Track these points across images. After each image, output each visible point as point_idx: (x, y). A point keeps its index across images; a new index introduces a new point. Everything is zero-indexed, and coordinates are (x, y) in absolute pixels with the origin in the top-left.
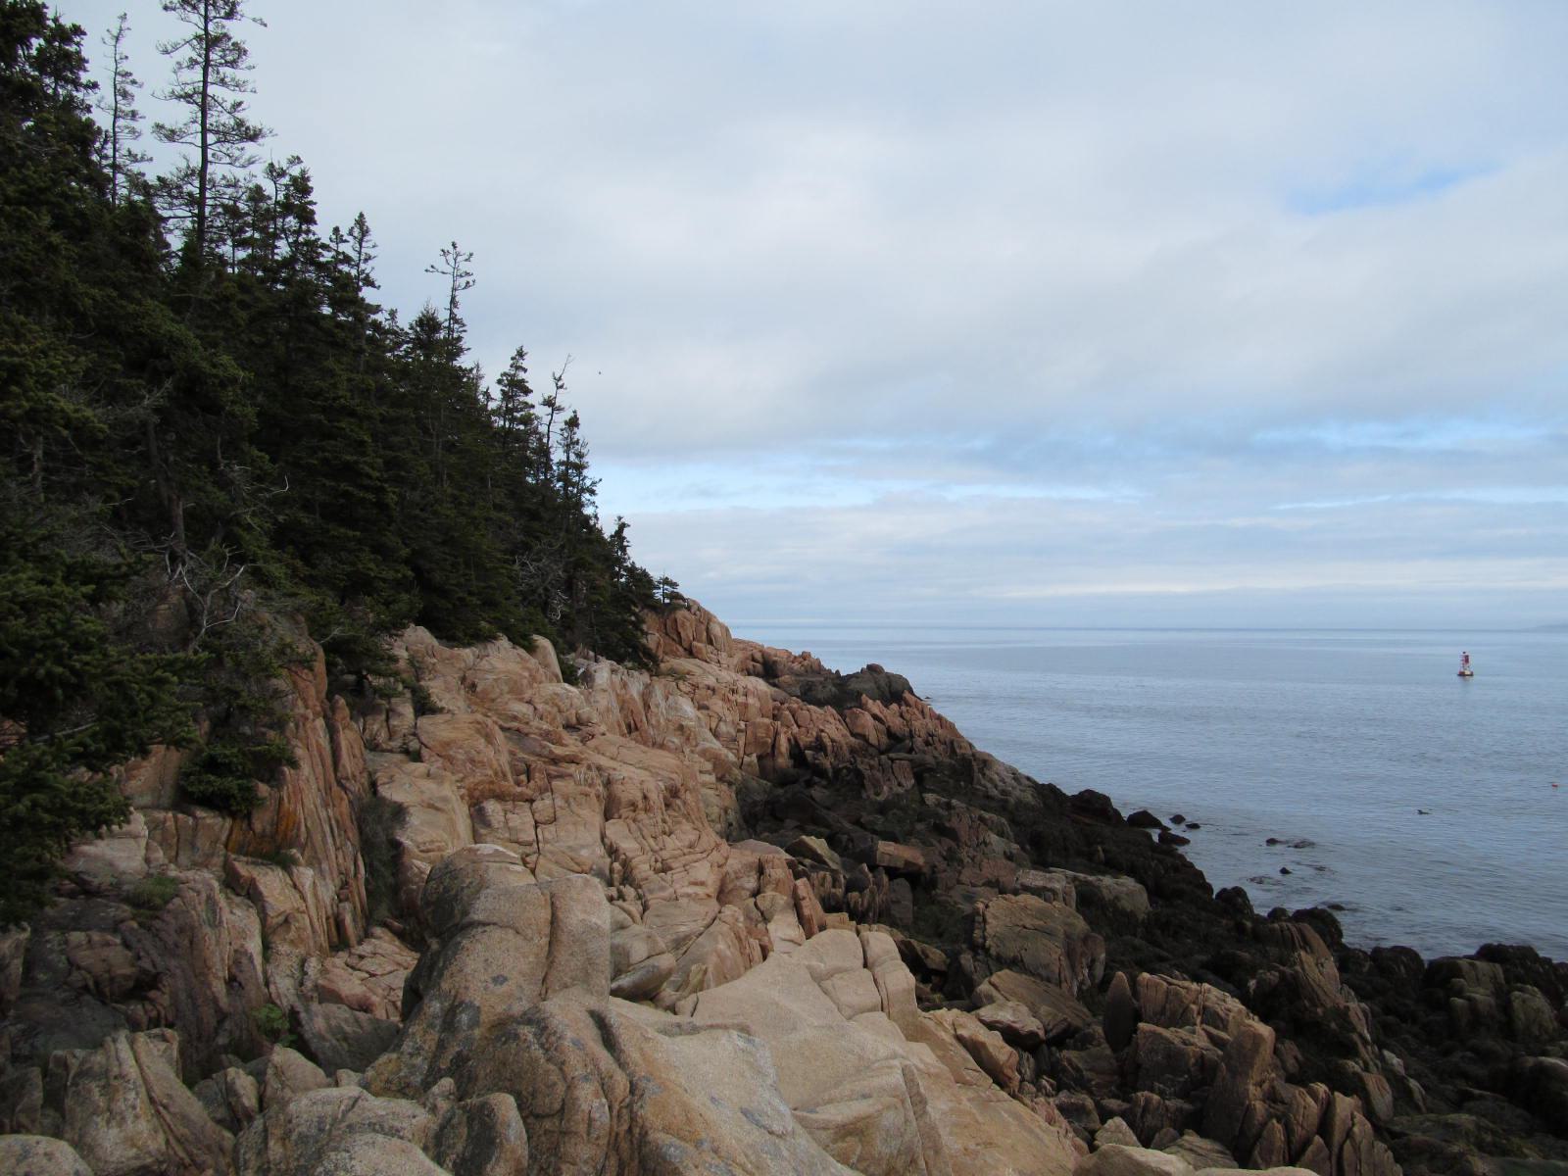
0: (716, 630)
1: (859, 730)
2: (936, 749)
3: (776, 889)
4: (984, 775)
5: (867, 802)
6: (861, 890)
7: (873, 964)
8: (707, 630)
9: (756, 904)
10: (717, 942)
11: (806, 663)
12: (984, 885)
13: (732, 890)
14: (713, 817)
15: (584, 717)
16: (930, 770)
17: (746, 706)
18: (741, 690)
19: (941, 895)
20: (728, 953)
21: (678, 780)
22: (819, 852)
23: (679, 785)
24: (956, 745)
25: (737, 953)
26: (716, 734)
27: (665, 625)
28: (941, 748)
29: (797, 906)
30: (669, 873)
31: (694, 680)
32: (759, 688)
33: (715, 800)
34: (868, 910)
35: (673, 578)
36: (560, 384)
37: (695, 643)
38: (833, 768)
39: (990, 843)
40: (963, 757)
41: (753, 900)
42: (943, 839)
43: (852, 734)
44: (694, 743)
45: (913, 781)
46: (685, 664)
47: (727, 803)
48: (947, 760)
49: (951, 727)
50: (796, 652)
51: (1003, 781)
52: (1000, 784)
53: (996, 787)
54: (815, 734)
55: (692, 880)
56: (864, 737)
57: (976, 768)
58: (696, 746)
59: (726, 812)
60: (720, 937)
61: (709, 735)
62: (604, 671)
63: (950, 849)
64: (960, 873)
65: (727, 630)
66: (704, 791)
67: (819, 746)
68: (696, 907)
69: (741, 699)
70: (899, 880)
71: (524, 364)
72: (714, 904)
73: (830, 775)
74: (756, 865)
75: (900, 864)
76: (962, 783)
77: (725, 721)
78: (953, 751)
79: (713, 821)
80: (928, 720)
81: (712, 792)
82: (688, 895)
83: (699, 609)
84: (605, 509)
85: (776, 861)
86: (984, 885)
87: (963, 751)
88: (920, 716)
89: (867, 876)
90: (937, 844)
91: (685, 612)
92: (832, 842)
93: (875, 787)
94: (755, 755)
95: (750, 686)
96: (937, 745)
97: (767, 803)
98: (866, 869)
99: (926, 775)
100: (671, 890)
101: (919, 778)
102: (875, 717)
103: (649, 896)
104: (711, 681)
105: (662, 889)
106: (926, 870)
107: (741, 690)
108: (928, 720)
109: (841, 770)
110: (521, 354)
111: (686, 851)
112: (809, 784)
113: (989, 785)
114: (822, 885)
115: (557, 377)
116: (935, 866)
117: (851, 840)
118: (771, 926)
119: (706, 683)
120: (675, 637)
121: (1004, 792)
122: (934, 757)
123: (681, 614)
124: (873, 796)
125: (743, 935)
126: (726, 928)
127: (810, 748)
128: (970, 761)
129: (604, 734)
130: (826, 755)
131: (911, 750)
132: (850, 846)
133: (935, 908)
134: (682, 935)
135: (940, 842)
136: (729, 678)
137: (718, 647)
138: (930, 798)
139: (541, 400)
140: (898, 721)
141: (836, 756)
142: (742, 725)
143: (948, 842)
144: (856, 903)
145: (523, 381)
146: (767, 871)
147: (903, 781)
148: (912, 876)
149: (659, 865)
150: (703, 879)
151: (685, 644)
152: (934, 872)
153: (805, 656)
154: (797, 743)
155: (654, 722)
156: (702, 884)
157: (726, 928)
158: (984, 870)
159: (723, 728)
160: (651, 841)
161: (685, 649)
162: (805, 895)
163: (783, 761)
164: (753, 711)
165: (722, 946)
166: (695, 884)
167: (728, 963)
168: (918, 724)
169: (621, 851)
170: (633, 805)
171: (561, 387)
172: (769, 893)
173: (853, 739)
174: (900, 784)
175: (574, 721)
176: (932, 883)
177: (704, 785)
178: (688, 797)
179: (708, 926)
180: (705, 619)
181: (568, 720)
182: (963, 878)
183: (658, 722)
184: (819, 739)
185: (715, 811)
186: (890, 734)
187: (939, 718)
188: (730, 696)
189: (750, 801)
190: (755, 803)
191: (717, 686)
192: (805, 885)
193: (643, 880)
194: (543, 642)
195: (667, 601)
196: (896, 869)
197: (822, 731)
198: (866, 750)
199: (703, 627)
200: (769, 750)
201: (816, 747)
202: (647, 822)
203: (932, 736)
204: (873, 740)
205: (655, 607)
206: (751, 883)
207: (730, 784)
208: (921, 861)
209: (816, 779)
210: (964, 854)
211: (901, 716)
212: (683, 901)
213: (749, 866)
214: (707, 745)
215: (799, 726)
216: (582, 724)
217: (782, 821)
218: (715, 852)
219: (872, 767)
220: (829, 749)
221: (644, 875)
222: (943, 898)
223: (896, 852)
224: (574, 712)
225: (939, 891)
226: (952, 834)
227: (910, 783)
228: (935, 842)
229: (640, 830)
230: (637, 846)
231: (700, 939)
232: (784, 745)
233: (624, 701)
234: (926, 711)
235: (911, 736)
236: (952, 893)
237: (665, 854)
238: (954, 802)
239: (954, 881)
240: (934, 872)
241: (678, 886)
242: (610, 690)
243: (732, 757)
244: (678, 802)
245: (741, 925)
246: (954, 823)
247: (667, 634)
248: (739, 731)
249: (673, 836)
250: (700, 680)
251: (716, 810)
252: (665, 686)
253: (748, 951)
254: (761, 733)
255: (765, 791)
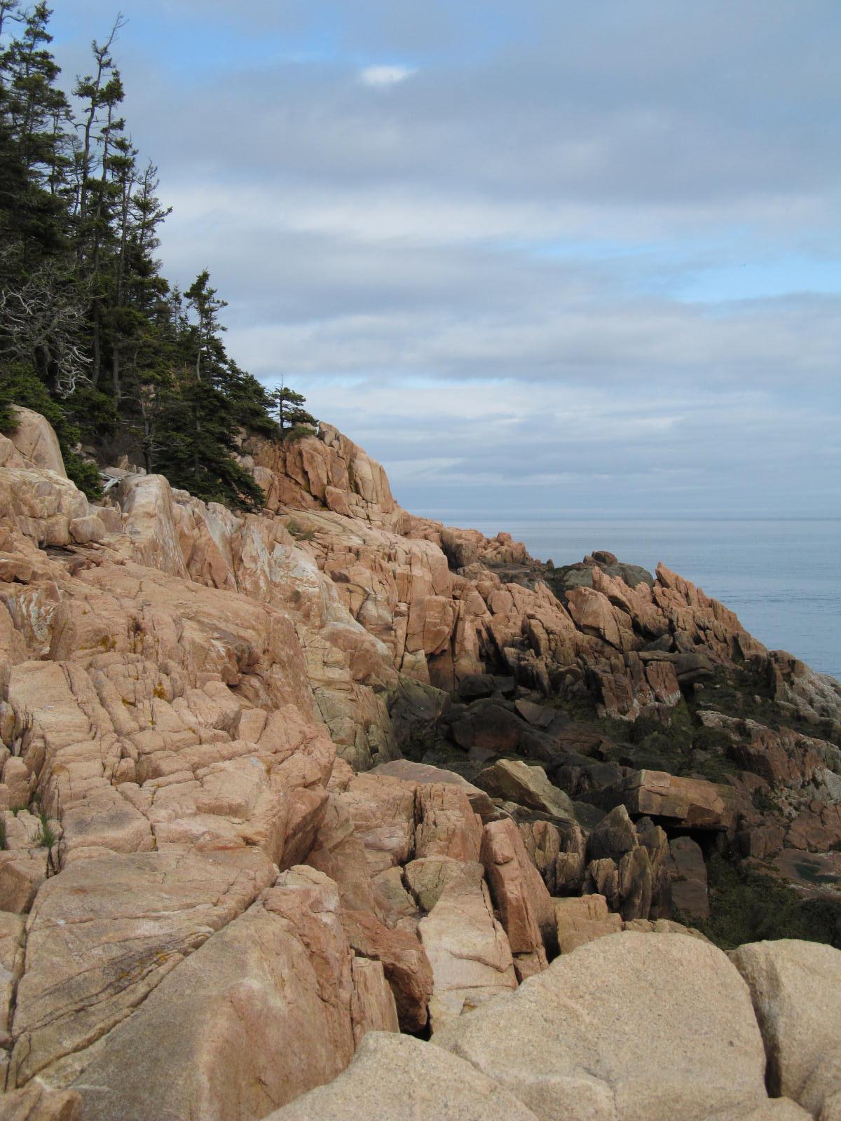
0: (364, 470)
1: (589, 621)
2: (711, 648)
3: (445, 851)
4: (792, 684)
5: (608, 723)
6: (618, 856)
7: (808, 1079)
8: (350, 468)
9: (404, 880)
10: (242, 967)
11: (503, 549)
12: (831, 848)
13: (340, 845)
14: (343, 735)
15: (85, 530)
16: (706, 678)
17: (409, 579)
18: (402, 557)
19: (758, 867)
20: (277, 1003)
21: (257, 641)
22: (532, 788)
23: (258, 651)
24: (741, 642)
25: (309, 1003)
26: (360, 618)
27: (285, 461)
28: (718, 647)
29: (492, 880)
30: (149, 784)
31: (328, 541)
32: (429, 552)
33: (345, 708)
34: (632, 893)
35: (296, 389)
36: (105, 59)
37: (330, 488)
38: (550, 674)
39: (824, 782)
40: (757, 660)
41: (398, 871)
42: (745, 773)
43: (578, 627)
44: (317, 623)
45: (678, 694)
46: (313, 518)
47: (369, 713)
48: (729, 665)
49: (732, 619)
50: (491, 535)
51: (822, 693)
52: (817, 698)
53: (811, 702)
54: (520, 623)
55: (206, 799)
56: (597, 631)
57: (778, 673)
58: (322, 627)
59: (366, 726)
60: (253, 956)
61: (345, 614)
62: (150, 489)
63: (758, 791)
64: (788, 828)
65: (381, 471)
66: (328, 693)
67: (528, 640)
68: (200, 870)
69: (401, 569)
70: (680, 840)
71: (49, 29)
72: (260, 863)
73: (546, 682)
74: (408, 803)
75: (681, 812)
76: (758, 698)
77: (375, 600)
78: (738, 653)
79: (341, 742)
80: (695, 606)
81: (342, 695)
82: (188, 839)
83: (337, 438)
84: (174, 257)
85: (449, 796)
86: (831, 848)
87: (753, 652)
88: (683, 601)
89: (627, 829)
90: (737, 782)
91: (313, 441)
92: (556, 776)
93: (618, 697)
94: (422, 652)
95: (416, 550)
96: (713, 642)
97: (443, 720)
98: (626, 817)
99: (697, 685)
100: (140, 824)
101: (687, 690)
102: (615, 601)
103: (72, 839)
104: (356, 542)
105: (118, 819)
106: (727, 822)
107: (402, 557)
108: (695, 606)
109: (563, 675)
110: (42, 14)
111: (205, 733)
112: (510, 696)
113: (799, 700)
114: (541, 846)
115: (100, 46)
116: (741, 817)
117: (587, 775)
118: (427, 925)
119: (345, 543)
120: (300, 479)
121: (824, 711)
122: (711, 660)
123: (307, 444)
124: (616, 716)
125: (334, 948)
126: (276, 926)
127: (512, 646)
128: (769, 662)
129: (122, 563)
130: (538, 654)
131: (673, 648)
132: (586, 786)
133: (749, 892)
134: (139, 947)
135: (740, 778)
136: (382, 540)
137: (368, 498)
138: (711, 718)
139: (76, 87)
140: (651, 608)
141: (554, 657)
142: (403, 607)
143: (753, 780)
144: (608, 879)
145: (45, 55)
146: (429, 816)
147: (663, 693)
148: (705, 835)
149: (128, 764)
150: (238, 800)
151: (315, 491)
152: (740, 827)
153: (501, 541)
154: (492, 639)
155: (248, 585)
156: (234, 811)
157: (276, 926)
158: (830, 823)
159: (371, 610)
160: (122, 712)
161: (315, 497)
162: (508, 852)
163: (469, 664)
164: (420, 590)
165: (253, 982)
166: (216, 810)
167: (274, 1035)
168: (684, 614)
169: (37, 730)
170: (106, 642)
171: (108, 64)
172: (432, 858)
173: (579, 633)
174: (657, 699)
175: (62, 535)
176: (742, 846)
177: (329, 683)
178: (277, 674)
179: (221, 923)
180: (348, 454)
181: (49, 531)
182: (794, 837)
183: (256, 584)
184: (526, 630)
185: (346, 725)
186: (636, 626)
187: (712, 604)
188: (385, 564)
189: (413, 718)
190: (421, 723)
191: (362, 548)
192: (510, 832)
193: (73, 797)
194: (32, 421)
195: (287, 425)
196: (676, 820)
197: (531, 617)
198: (601, 653)
199: (344, 466)
200: (446, 646)
201: (522, 643)
202: (120, 668)
203: (704, 629)
204: (611, 635)
205: (268, 431)
206: (398, 838)
207: (378, 689)
208: (719, 806)
209: (523, 690)
210: (785, 798)
211: (655, 602)
212: (169, 854)
213: (393, 806)
214: (340, 626)
215: (493, 613)
216: (77, 544)
217: (466, 751)
218: (298, 755)
219: (613, 669)
220: (543, 644)
221: (79, 786)
222: (763, 872)
223: (673, 791)
224: (62, 520)
225: (751, 859)
226: (759, 765)
227: (673, 697)
228: (734, 779)
229: (98, 687)
230: (80, 718)
231: (191, 961)
232: (469, 632)
233: (195, 549)
234: (692, 594)
235: (671, 629)
236: (776, 863)
237: (147, 740)
238: (750, 722)
239: (779, 843)
240: (740, 827)
241: (163, 813)
242: (162, 516)
243: (382, 648)
244: (255, 682)
245: (327, 919)
246: (755, 748)
247: (287, 475)
248: (397, 614)
249: (180, 701)
250: (335, 540)
251: (348, 723)
252: (269, 528)
253: (345, 995)
254: (433, 616)
255: (438, 705)
